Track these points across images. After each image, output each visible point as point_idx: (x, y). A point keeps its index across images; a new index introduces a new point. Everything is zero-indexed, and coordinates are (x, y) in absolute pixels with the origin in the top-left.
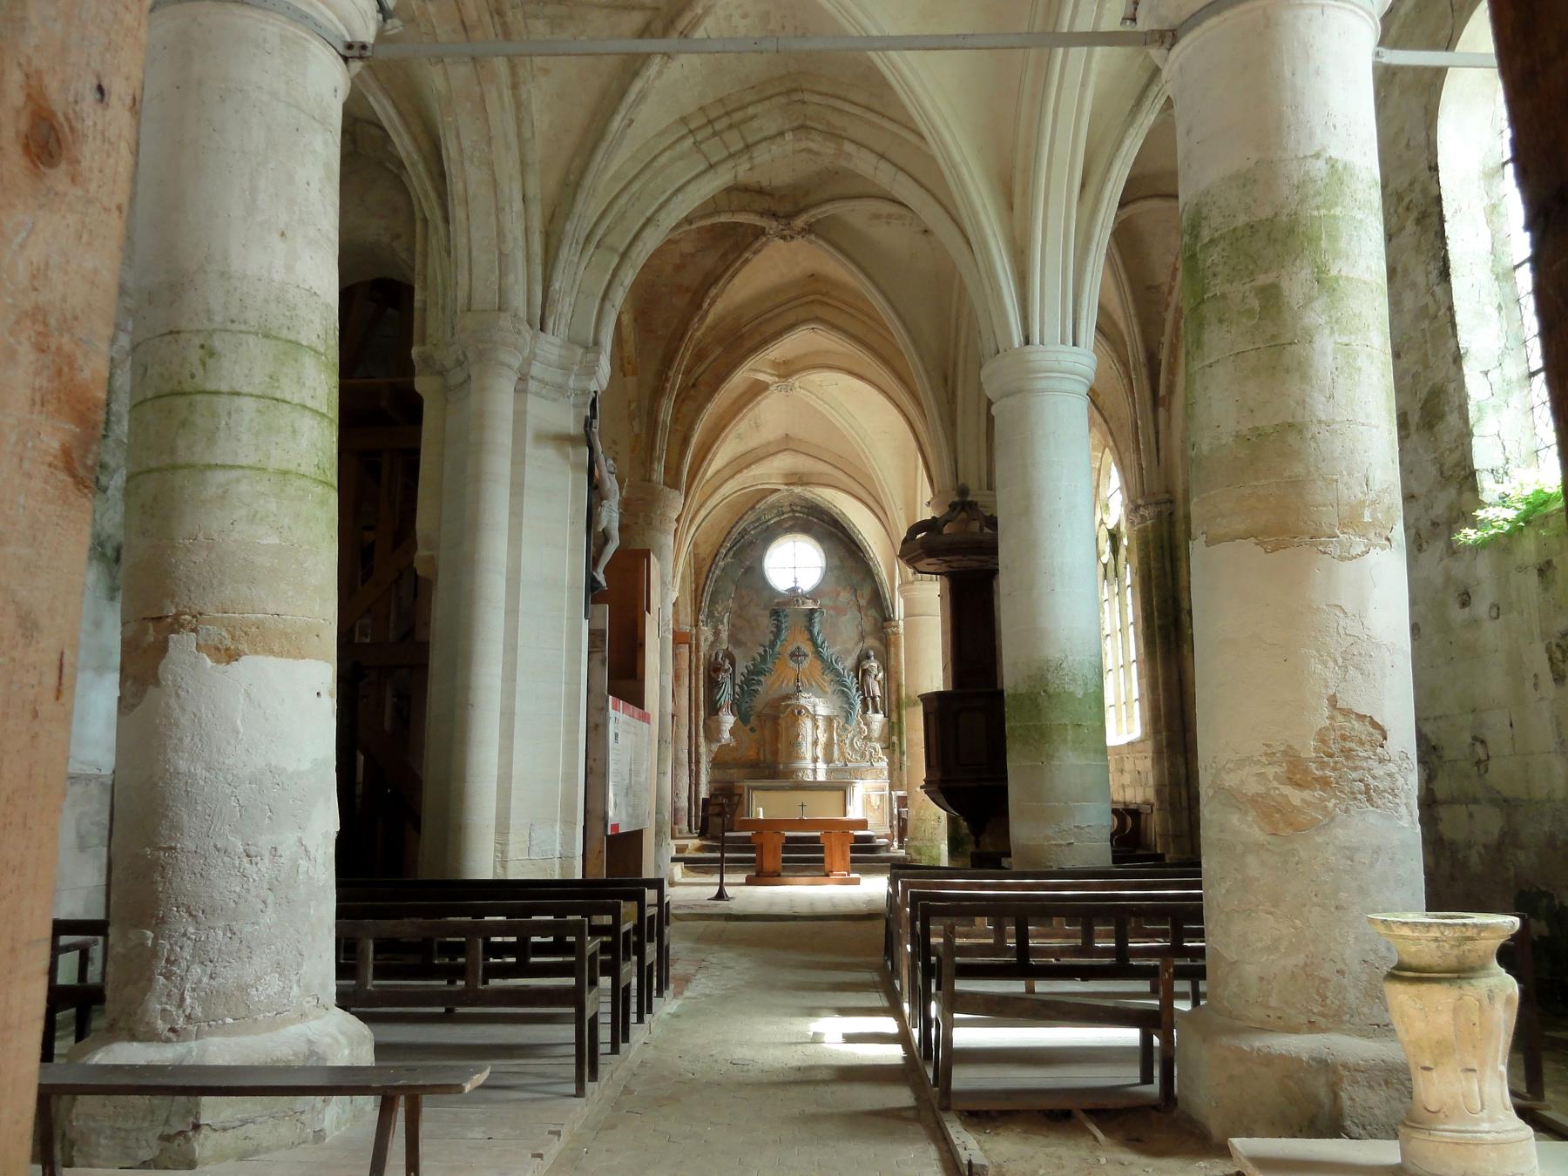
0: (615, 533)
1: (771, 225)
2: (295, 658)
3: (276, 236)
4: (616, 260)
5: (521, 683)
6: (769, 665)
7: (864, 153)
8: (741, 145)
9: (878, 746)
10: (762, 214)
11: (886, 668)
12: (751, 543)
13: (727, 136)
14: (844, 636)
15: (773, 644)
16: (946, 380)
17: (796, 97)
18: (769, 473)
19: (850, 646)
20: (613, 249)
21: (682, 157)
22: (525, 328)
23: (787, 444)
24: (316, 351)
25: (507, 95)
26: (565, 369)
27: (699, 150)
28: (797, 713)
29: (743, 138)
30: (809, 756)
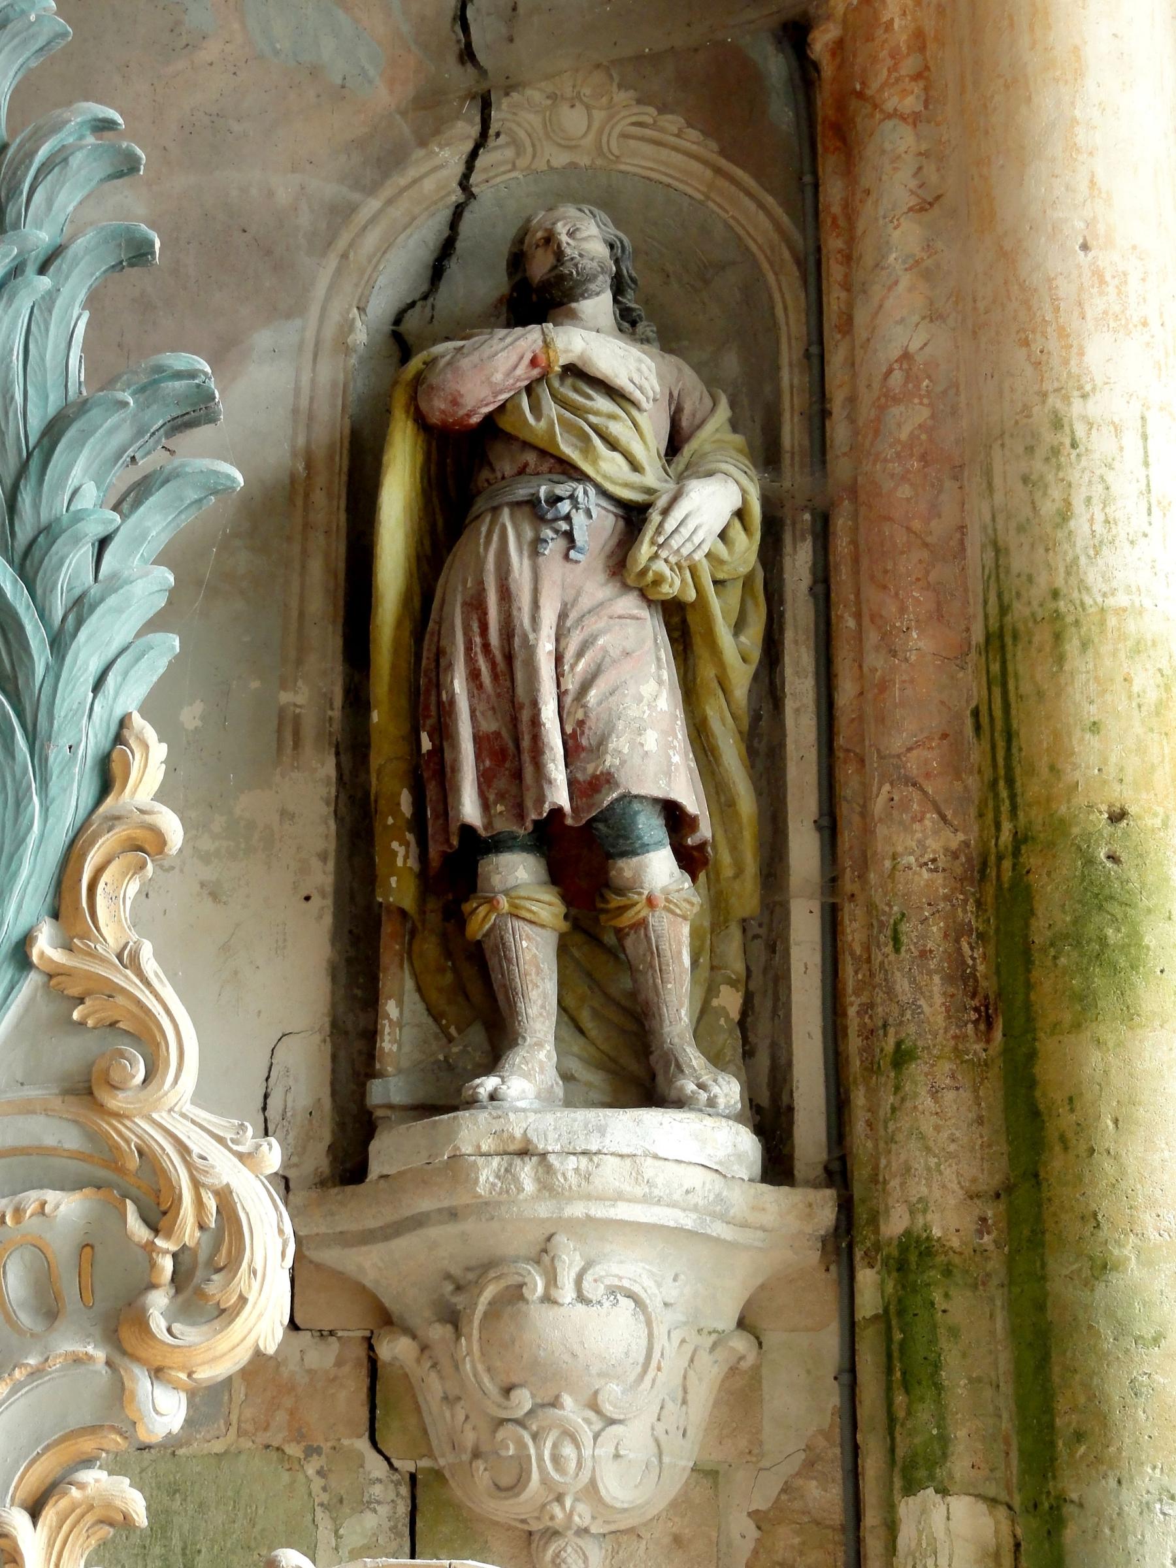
11: (780, 355)
19: (285, 175)
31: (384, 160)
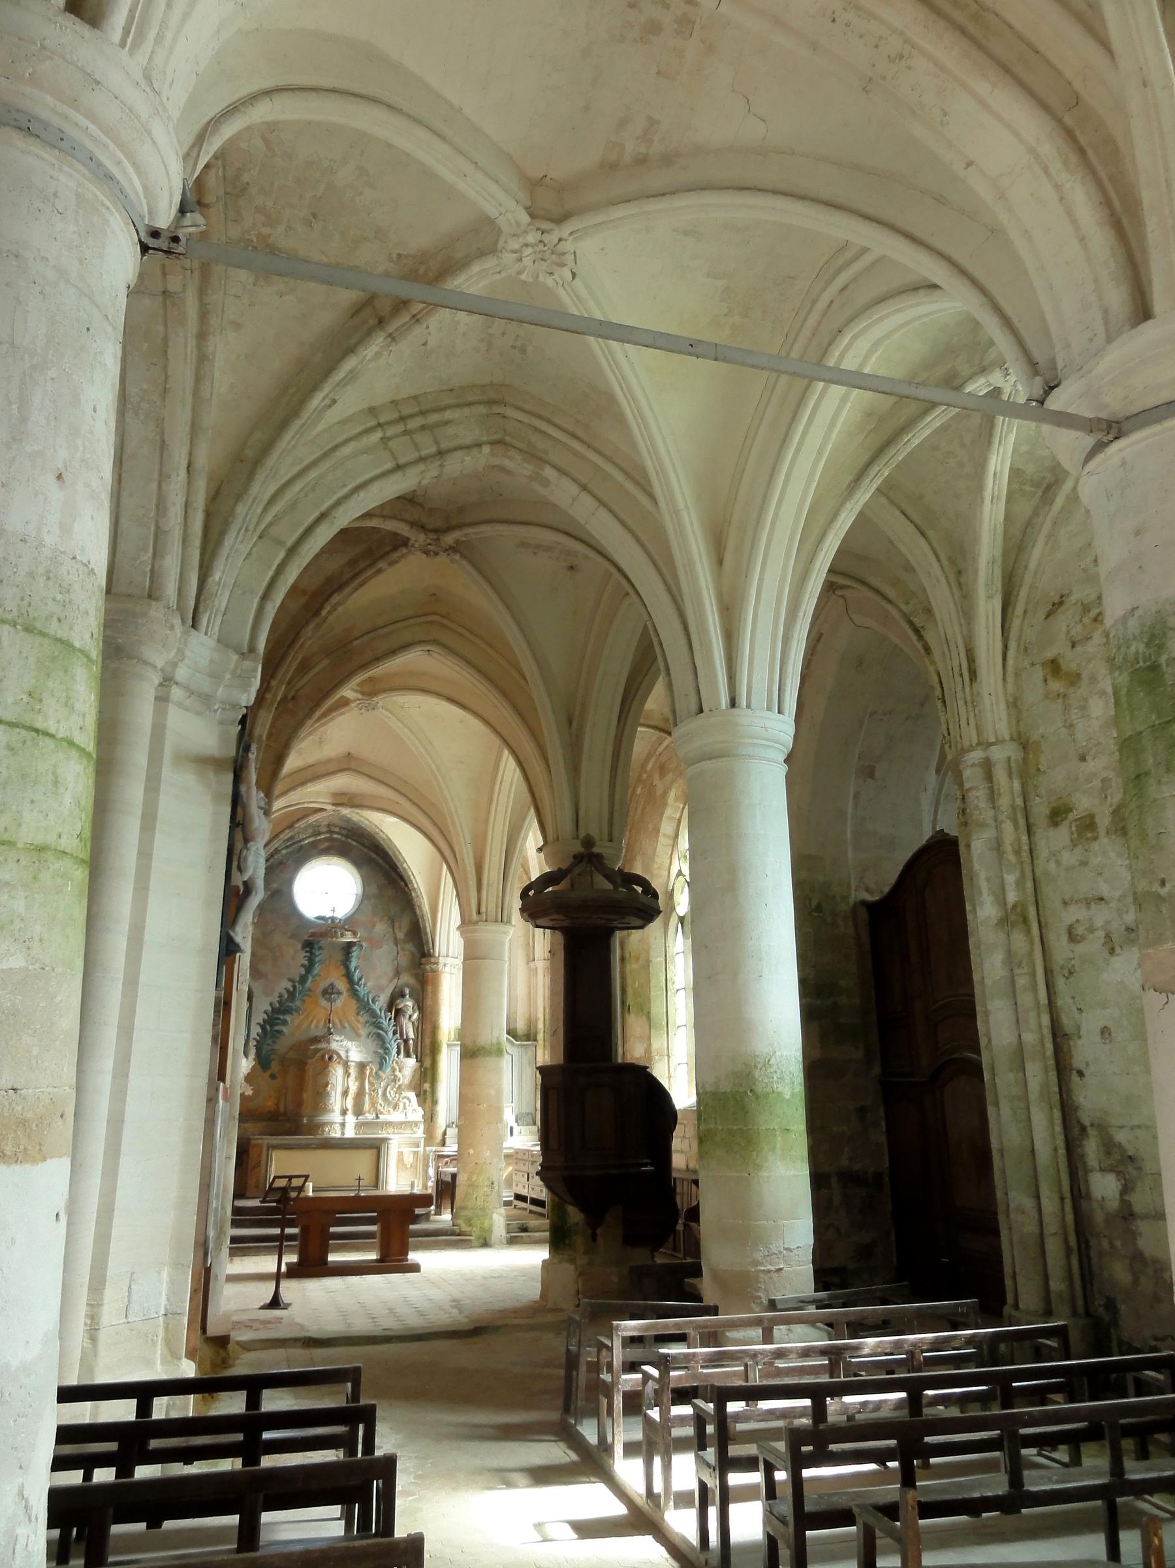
0: (260, 883)
1: (419, 538)
2: (35, 1161)
3: (51, 479)
4: (282, 555)
5: (136, 1080)
6: (298, 1003)
7: (566, 483)
8: (434, 450)
9: (412, 1095)
10: (412, 524)
11: (420, 1006)
12: (281, 863)
13: (418, 437)
14: (378, 971)
15: (303, 979)
16: (570, 722)
17: (497, 409)
18: (316, 795)
20: (279, 542)
21: (367, 451)
22: (177, 621)
23: (348, 763)
24: (88, 657)
25: (192, 342)
26: (216, 676)
27: (386, 448)
28: (327, 1059)
29: (437, 443)
30: (337, 1107)
31: (391, 980)
